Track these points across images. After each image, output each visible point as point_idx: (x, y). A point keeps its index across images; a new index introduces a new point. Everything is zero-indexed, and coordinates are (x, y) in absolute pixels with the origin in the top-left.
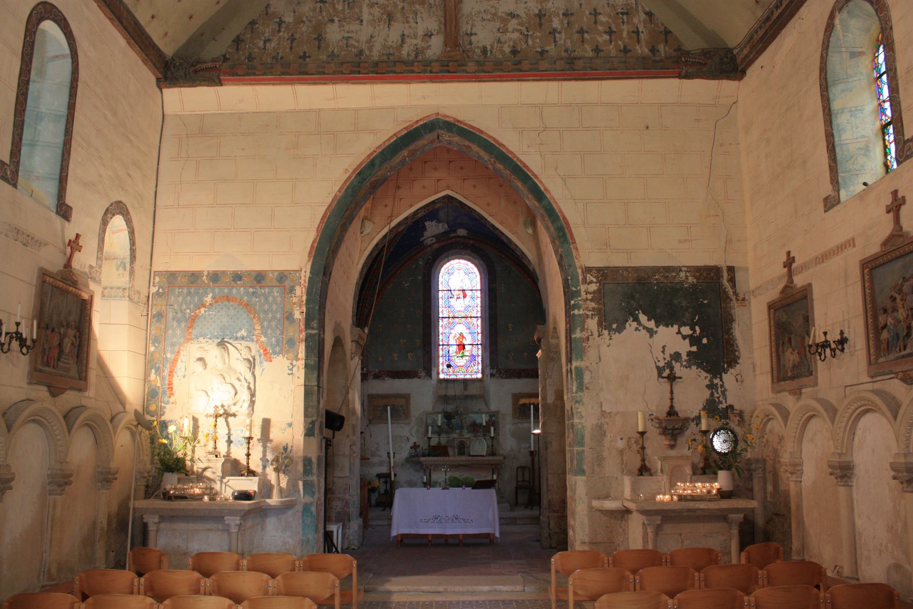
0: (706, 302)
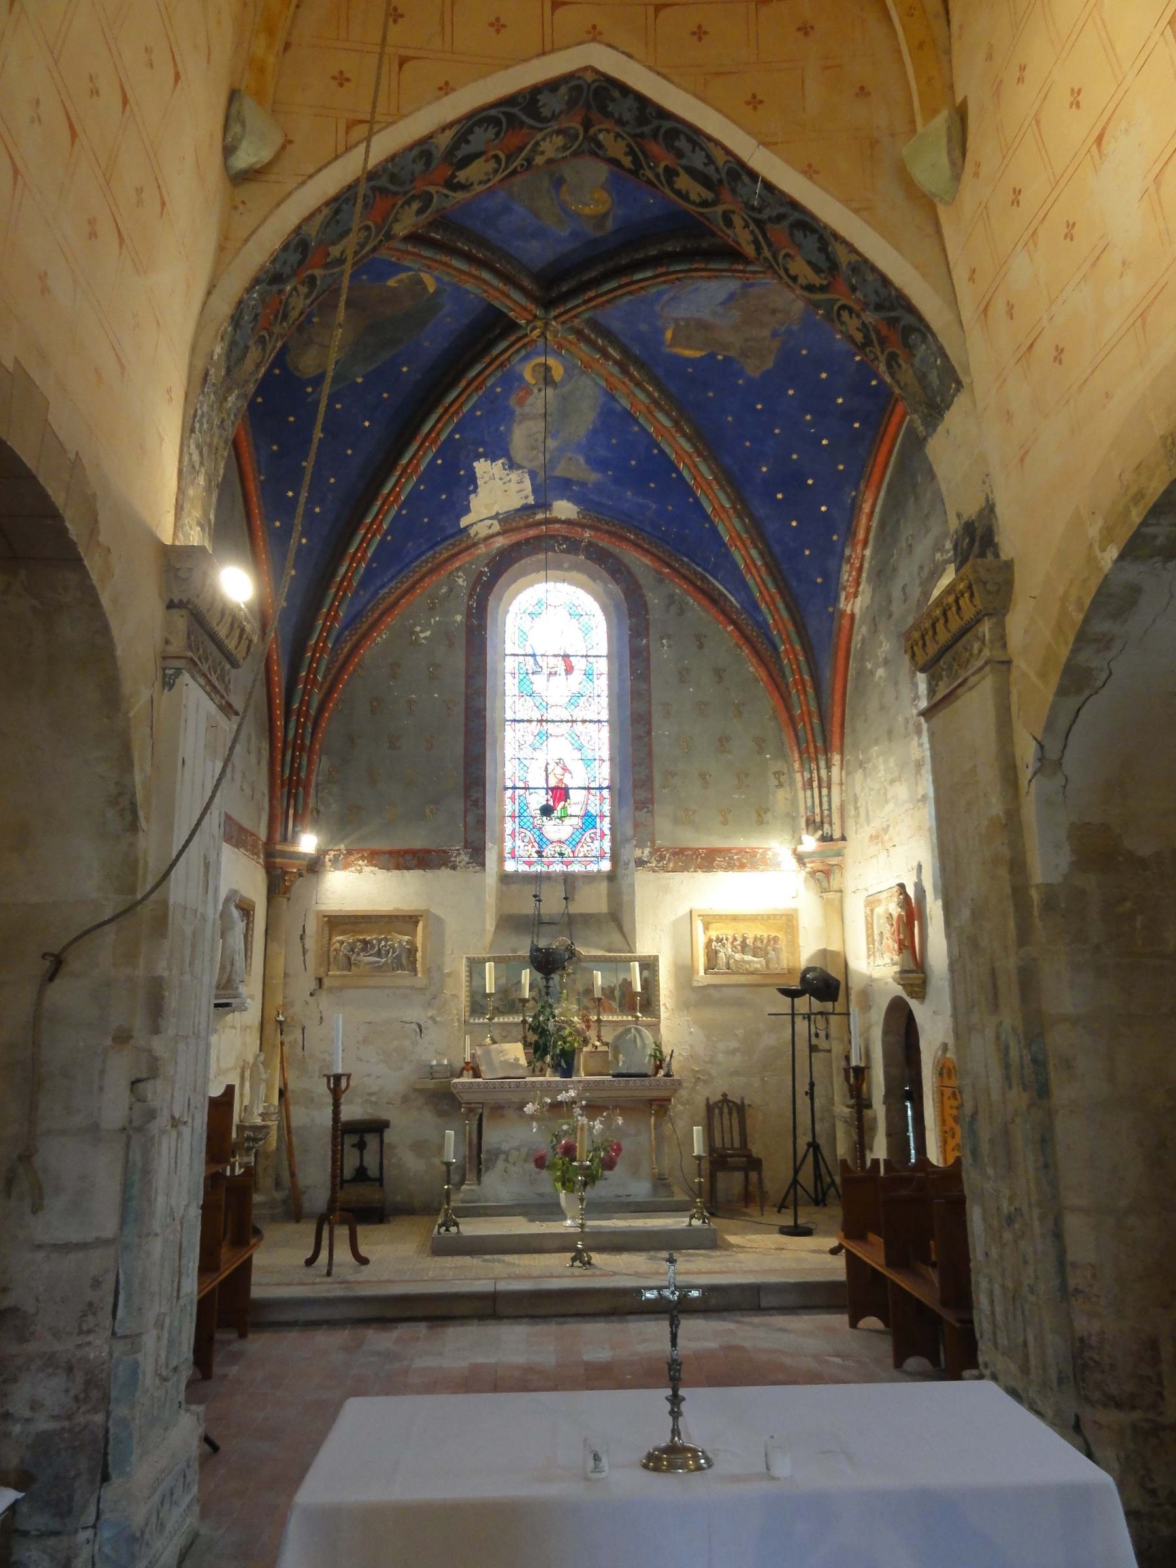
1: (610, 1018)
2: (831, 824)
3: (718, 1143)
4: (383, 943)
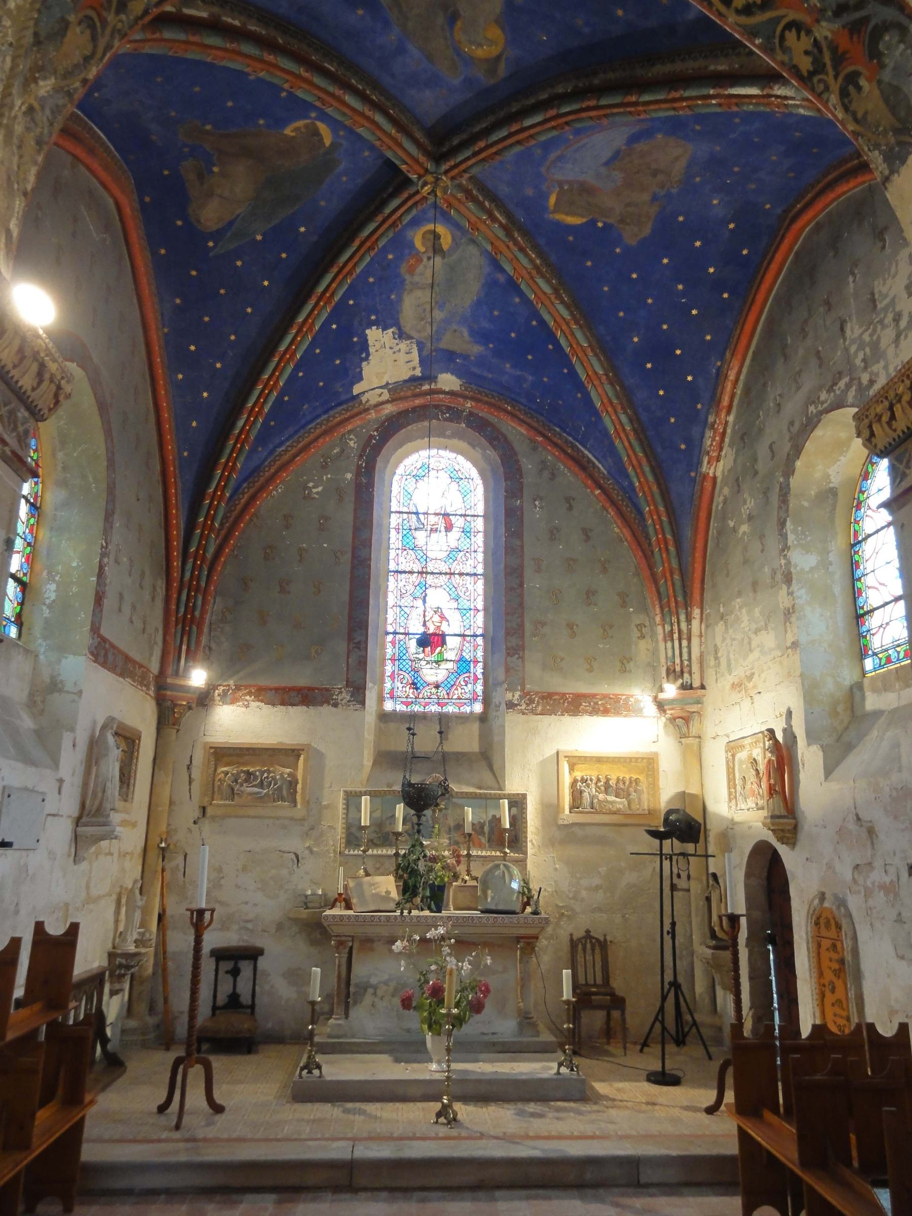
1: (479, 853)
2: (690, 673)
3: (582, 980)
4: (266, 775)
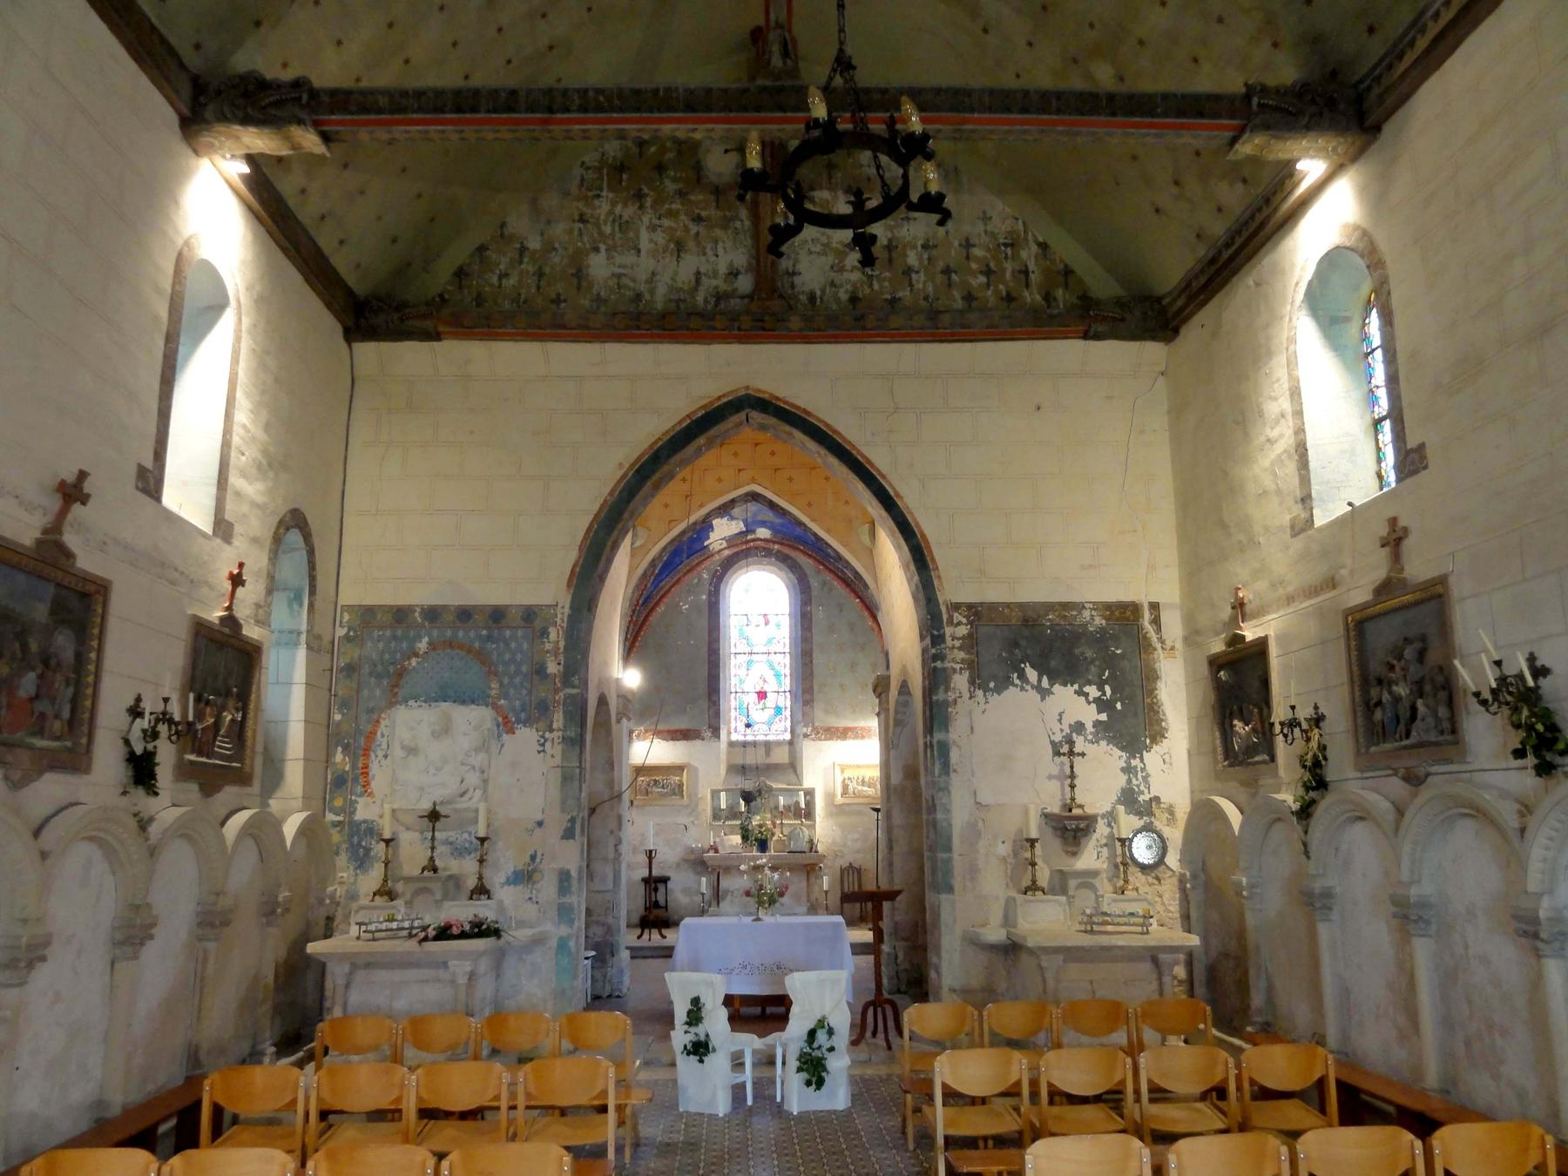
0: (1119, 652)
3: (846, 889)
